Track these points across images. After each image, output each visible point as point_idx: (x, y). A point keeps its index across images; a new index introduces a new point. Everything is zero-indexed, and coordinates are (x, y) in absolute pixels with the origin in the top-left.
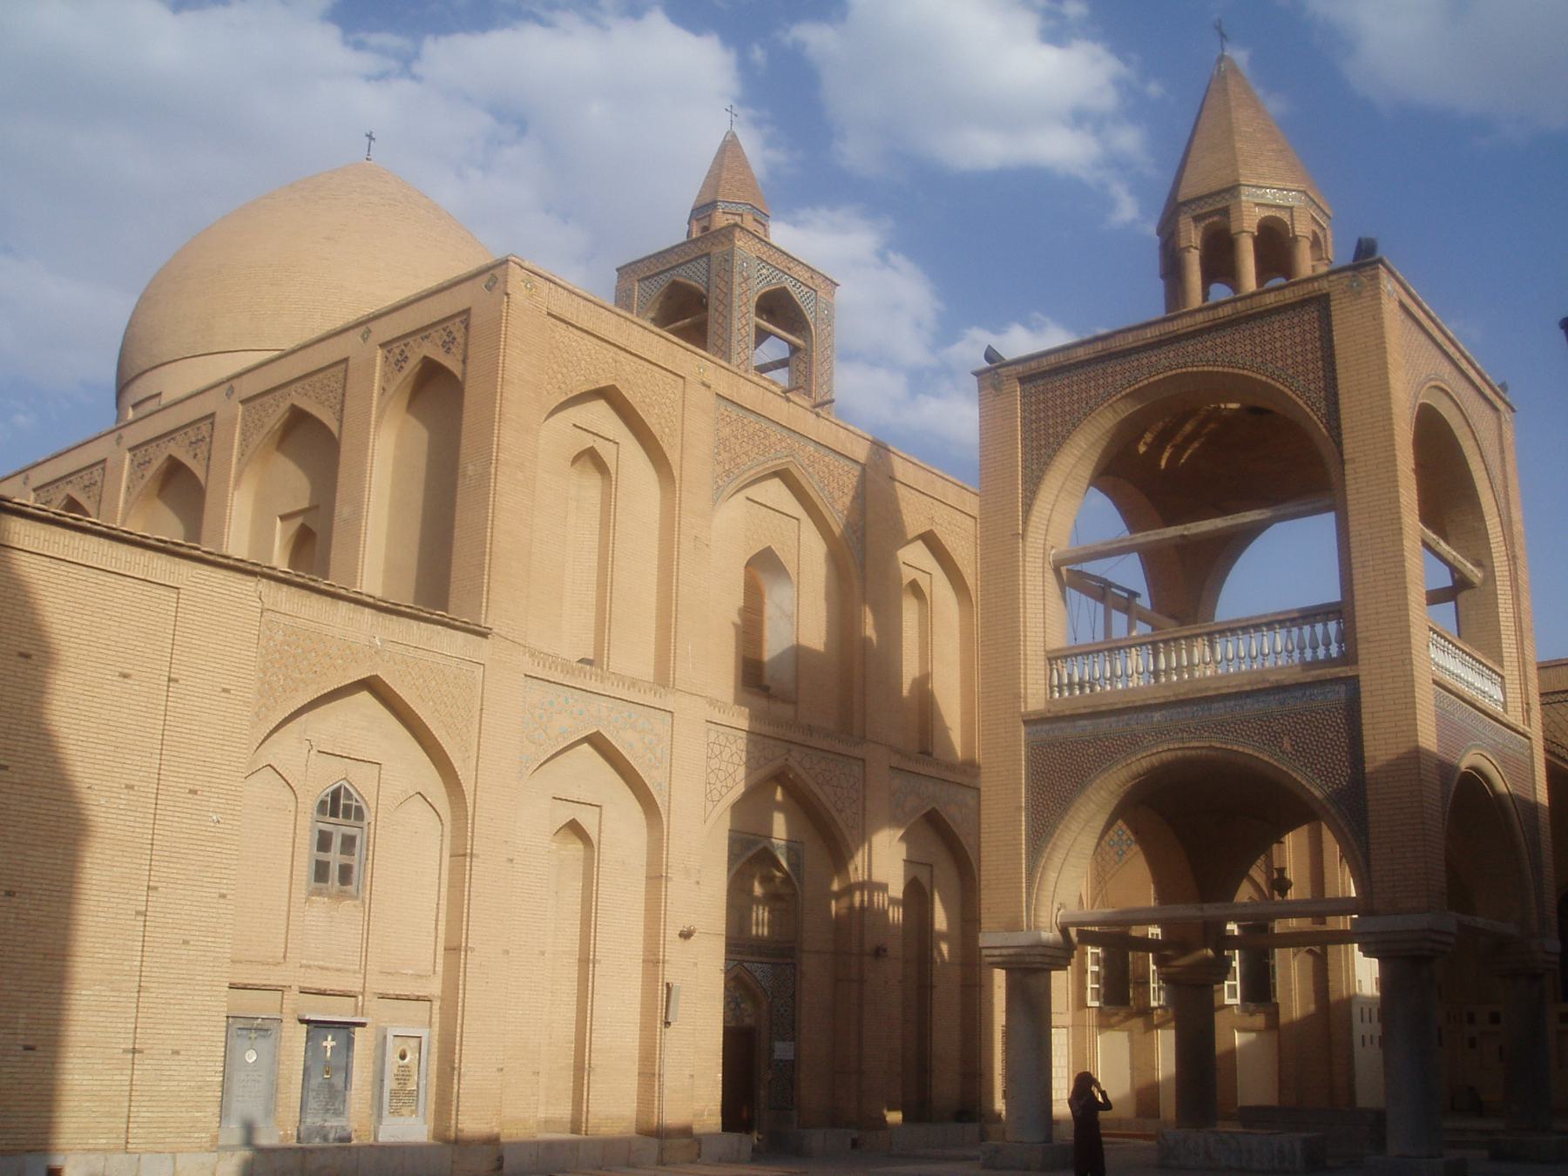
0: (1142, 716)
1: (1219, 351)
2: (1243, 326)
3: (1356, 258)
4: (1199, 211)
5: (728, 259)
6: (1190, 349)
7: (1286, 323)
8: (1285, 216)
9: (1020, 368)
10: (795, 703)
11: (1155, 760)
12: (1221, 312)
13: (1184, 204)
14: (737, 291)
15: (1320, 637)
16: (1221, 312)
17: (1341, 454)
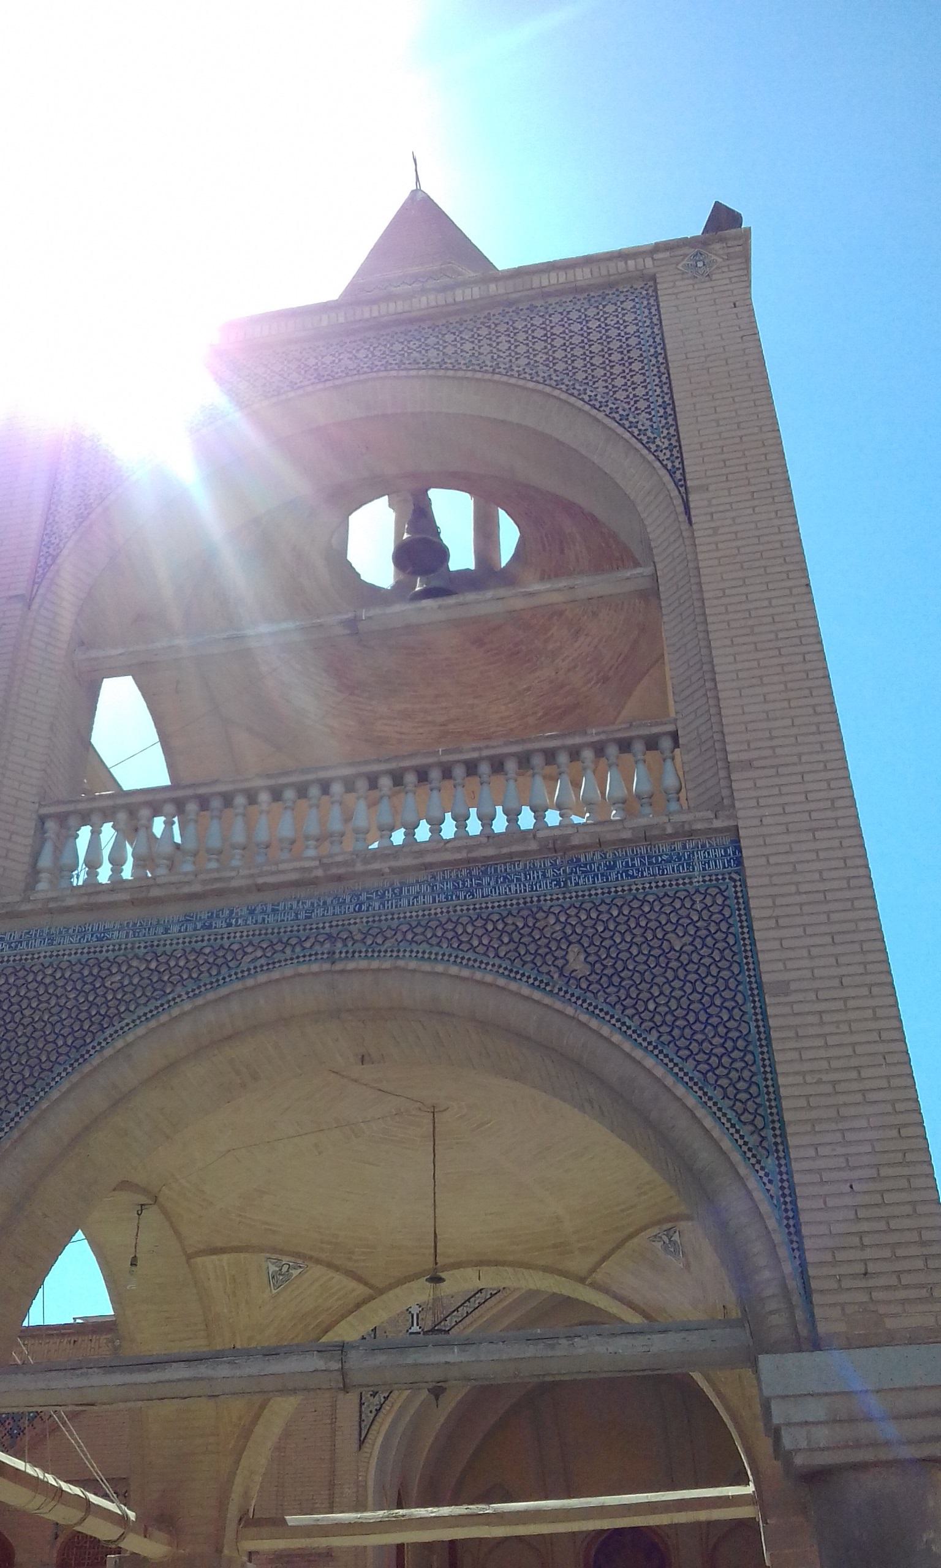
17: (681, 484)
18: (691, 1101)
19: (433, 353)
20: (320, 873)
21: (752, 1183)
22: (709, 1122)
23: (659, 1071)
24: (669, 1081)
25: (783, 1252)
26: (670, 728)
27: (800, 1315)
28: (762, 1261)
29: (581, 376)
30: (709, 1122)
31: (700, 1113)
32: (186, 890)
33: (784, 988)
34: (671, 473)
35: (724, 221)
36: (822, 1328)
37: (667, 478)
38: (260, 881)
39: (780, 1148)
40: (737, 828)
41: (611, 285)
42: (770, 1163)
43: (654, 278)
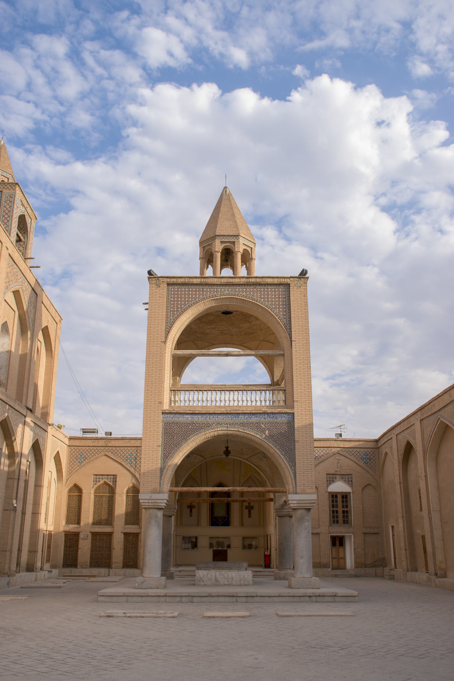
0: (212, 416)
1: (248, 293)
2: (258, 287)
3: (300, 275)
4: (223, 240)
5: (12, 197)
6: (237, 290)
7: (273, 290)
8: (249, 250)
9: (168, 280)
10: (6, 389)
11: (216, 434)
12: (251, 280)
13: (218, 236)
14: (15, 212)
15: (268, 398)
16: (251, 280)
17: (291, 338)
18: (283, 457)
19: (244, 293)
20: (225, 412)
21: (290, 470)
22: (285, 461)
23: (279, 453)
24: (280, 454)
25: (293, 480)
26: (284, 389)
27: (295, 489)
28: (290, 481)
29: (274, 306)
30: (285, 461)
31: (284, 459)
32: (202, 412)
33: (298, 441)
34: (289, 335)
35: (304, 273)
36: (297, 491)
37: (288, 336)
38: (215, 412)
39: (295, 466)
40: (294, 413)
41: (281, 284)
42: (293, 468)
43: (289, 284)
